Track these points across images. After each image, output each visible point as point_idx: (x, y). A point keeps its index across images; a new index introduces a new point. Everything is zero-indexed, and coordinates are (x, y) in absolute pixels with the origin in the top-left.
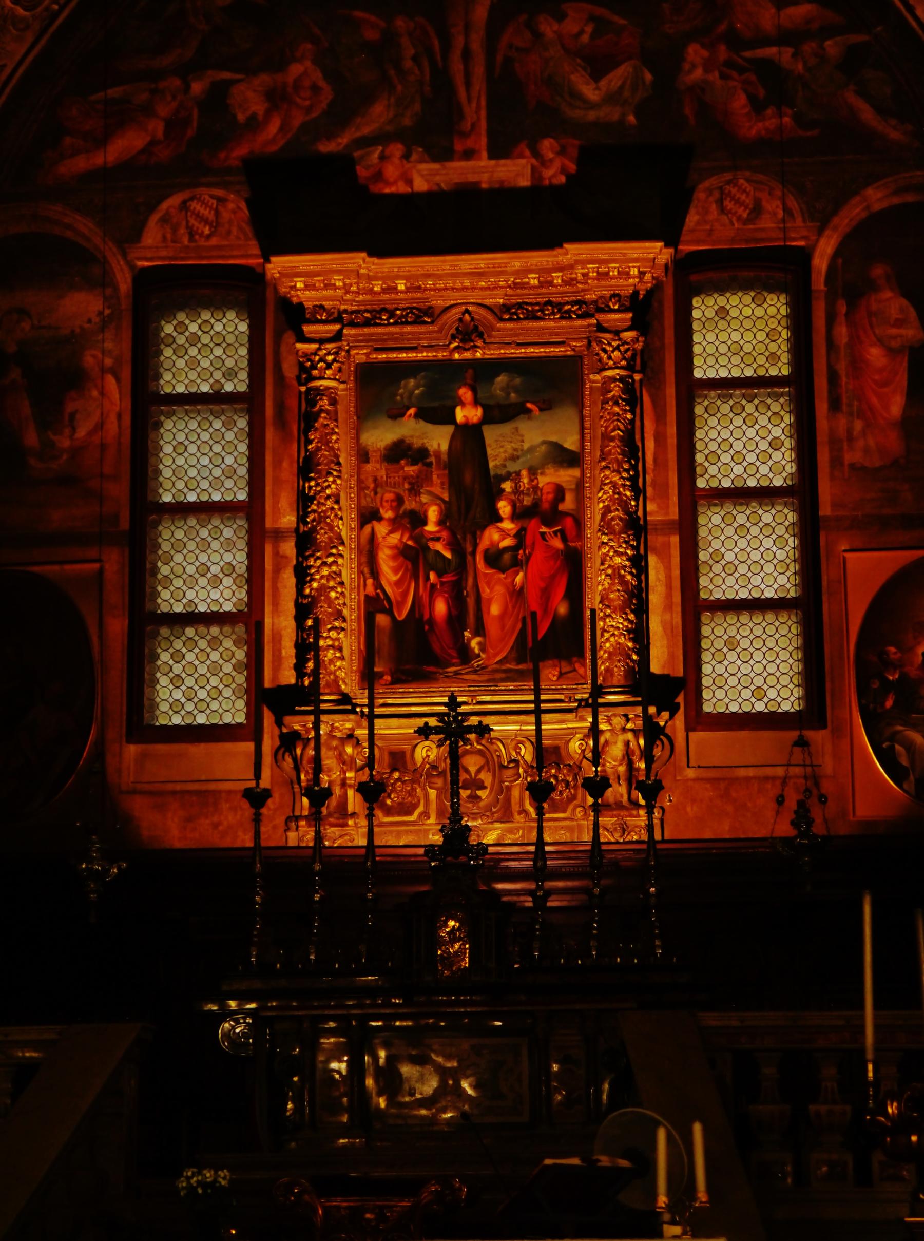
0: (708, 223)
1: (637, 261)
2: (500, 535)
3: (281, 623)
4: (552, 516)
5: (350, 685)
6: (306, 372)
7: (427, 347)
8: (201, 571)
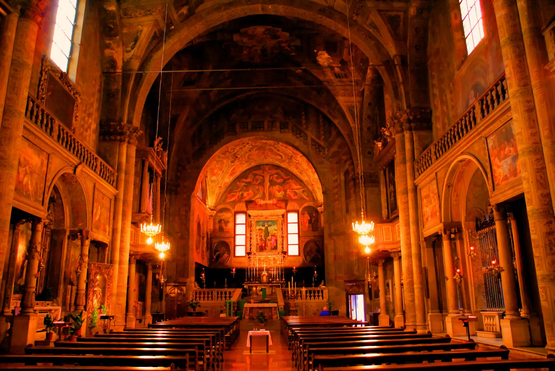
0: (289, 207)
1: (282, 211)
2: (269, 238)
3: (248, 246)
4: (274, 236)
5: (255, 252)
6: (251, 222)
7: (263, 219)
8: (240, 240)
